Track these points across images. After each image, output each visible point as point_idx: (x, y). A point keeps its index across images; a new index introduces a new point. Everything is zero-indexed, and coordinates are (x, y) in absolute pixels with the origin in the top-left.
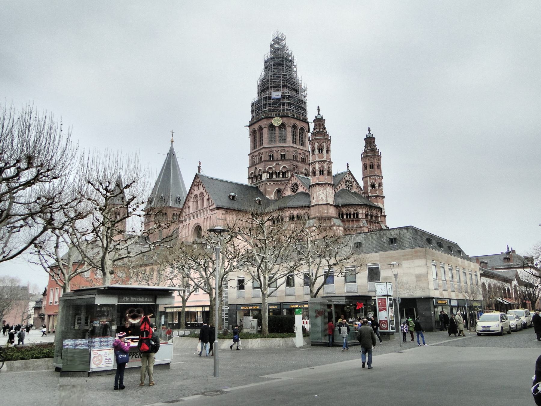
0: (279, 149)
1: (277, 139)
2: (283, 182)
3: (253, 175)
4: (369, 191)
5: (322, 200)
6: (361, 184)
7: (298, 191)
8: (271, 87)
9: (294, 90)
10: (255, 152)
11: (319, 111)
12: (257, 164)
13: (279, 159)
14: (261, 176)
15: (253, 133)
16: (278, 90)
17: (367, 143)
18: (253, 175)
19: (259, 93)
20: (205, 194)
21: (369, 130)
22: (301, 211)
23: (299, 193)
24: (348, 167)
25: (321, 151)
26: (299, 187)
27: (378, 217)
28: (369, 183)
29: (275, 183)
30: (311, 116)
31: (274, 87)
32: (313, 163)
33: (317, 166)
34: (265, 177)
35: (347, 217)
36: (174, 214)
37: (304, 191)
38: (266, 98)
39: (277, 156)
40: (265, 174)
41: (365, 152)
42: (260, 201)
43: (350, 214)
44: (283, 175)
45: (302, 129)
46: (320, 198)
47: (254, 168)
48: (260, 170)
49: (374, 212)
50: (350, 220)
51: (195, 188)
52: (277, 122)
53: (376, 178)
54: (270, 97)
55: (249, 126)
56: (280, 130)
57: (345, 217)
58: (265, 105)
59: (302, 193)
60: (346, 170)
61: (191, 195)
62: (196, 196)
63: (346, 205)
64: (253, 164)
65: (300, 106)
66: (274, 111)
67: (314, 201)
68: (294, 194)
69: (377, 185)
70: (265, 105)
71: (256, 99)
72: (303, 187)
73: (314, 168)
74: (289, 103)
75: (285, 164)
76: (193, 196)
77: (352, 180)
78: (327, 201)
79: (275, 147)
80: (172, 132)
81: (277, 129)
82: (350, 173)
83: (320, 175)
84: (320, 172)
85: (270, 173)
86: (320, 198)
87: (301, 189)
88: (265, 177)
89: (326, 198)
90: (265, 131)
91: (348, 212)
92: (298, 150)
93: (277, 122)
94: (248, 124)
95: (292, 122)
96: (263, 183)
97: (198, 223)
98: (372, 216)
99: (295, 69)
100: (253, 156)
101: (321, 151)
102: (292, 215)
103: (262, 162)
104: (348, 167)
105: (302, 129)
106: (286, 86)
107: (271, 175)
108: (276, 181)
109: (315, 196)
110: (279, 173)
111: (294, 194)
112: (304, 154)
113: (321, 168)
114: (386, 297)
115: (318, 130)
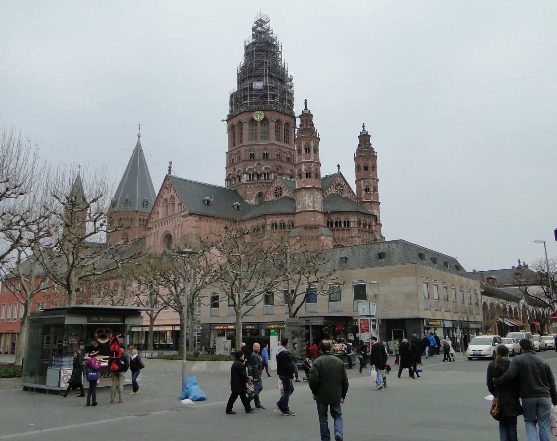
0: (261, 147)
1: (259, 136)
2: (265, 185)
3: (231, 176)
4: (363, 196)
5: (309, 206)
6: (354, 188)
7: (282, 196)
8: (252, 76)
9: (279, 79)
11: (306, 105)
12: (236, 164)
13: (261, 158)
14: (240, 177)
15: (232, 130)
16: (260, 80)
17: (360, 141)
18: (231, 176)
19: (239, 83)
20: (176, 198)
21: (364, 127)
22: (284, 218)
23: (283, 198)
24: (339, 168)
25: (308, 150)
26: (283, 191)
27: (372, 226)
28: (363, 187)
29: (256, 185)
30: (298, 111)
31: (256, 76)
32: (299, 164)
33: (303, 167)
34: (245, 178)
35: (336, 226)
36: (140, 219)
37: (289, 195)
38: (246, 89)
39: (259, 155)
40: (245, 175)
41: (359, 151)
42: (238, 207)
43: (340, 222)
44: (265, 176)
47: (232, 168)
48: (239, 170)
49: (368, 220)
50: (340, 228)
51: (165, 191)
53: (371, 181)
54: (251, 88)
55: (227, 121)
56: (262, 125)
57: (334, 226)
58: (246, 96)
59: (286, 198)
60: (336, 171)
62: (166, 200)
63: (336, 212)
64: (231, 164)
65: (286, 98)
66: (255, 103)
67: (299, 207)
68: (277, 199)
69: (372, 189)
70: (246, 96)
71: (236, 90)
72: (287, 190)
73: (300, 170)
74: (273, 95)
76: (163, 200)
77: (343, 183)
78: (314, 208)
79: (256, 145)
80: (139, 125)
81: (259, 124)
82: (340, 175)
83: (307, 177)
84: (307, 174)
85: (250, 175)
87: (285, 194)
88: (245, 178)
89: (314, 204)
90: (246, 127)
91: (338, 221)
92: (282, 149)
93: (259, 116)
94: (226, 118)
95: (277, 116)
96: (243, 186)
98: (365, 225)
99: (280, 56)
100: (231, 155)
101: (308, 150)
102: (274, 223)
103: (242, 161)
104: (339, 168)
105: (287, 124)
106: (269, 75)
107: (251, 176)
108: (257, 183)
109: (301, 202)
111: (277, 199)
112: (290, 153)
113: (308, 170)
114: (369, 318)
115: (305, 127)
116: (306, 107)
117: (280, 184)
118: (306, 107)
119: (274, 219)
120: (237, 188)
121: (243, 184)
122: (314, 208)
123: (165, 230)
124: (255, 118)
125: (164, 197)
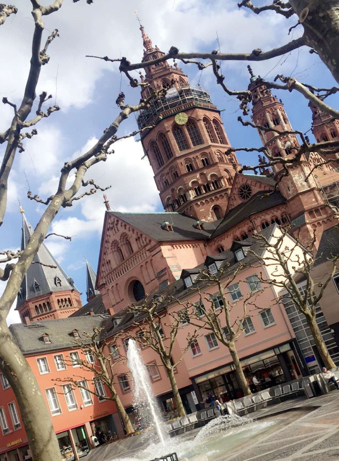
5: (303, 186)
10: (164, 168)
11: (251, 73)
12: (172, 184)
20: (130, 233)
22: (275, 213)
26: (253, 188)
34: (192, 195)
45: (215, 121)
46: (299, 185)
47: (169, 191)
48: (180, 189)
51: (110, 233)
52: (182, 119)
61: (106, 245)
62: (115, 243)
67: (290, 192)
75: (213, 171)
76: (110, 245)
78: (309, 186)
86: (299, 185)
88: (192, 195)
95: (201, 114)
97: (132, 277)
100: (162, 176)
102: (264, 222)
108: (208, 196)
109: (290, 185)
110: (207, 185)
116: (252, 75)
117: (244, 182)
118: (252, 75)
119: (263, 217)
120: (185, 209)
121: (192, 202)
122: (309, 186)
123: (126, 278)
124: (178, 122)
125: (111, 240)
